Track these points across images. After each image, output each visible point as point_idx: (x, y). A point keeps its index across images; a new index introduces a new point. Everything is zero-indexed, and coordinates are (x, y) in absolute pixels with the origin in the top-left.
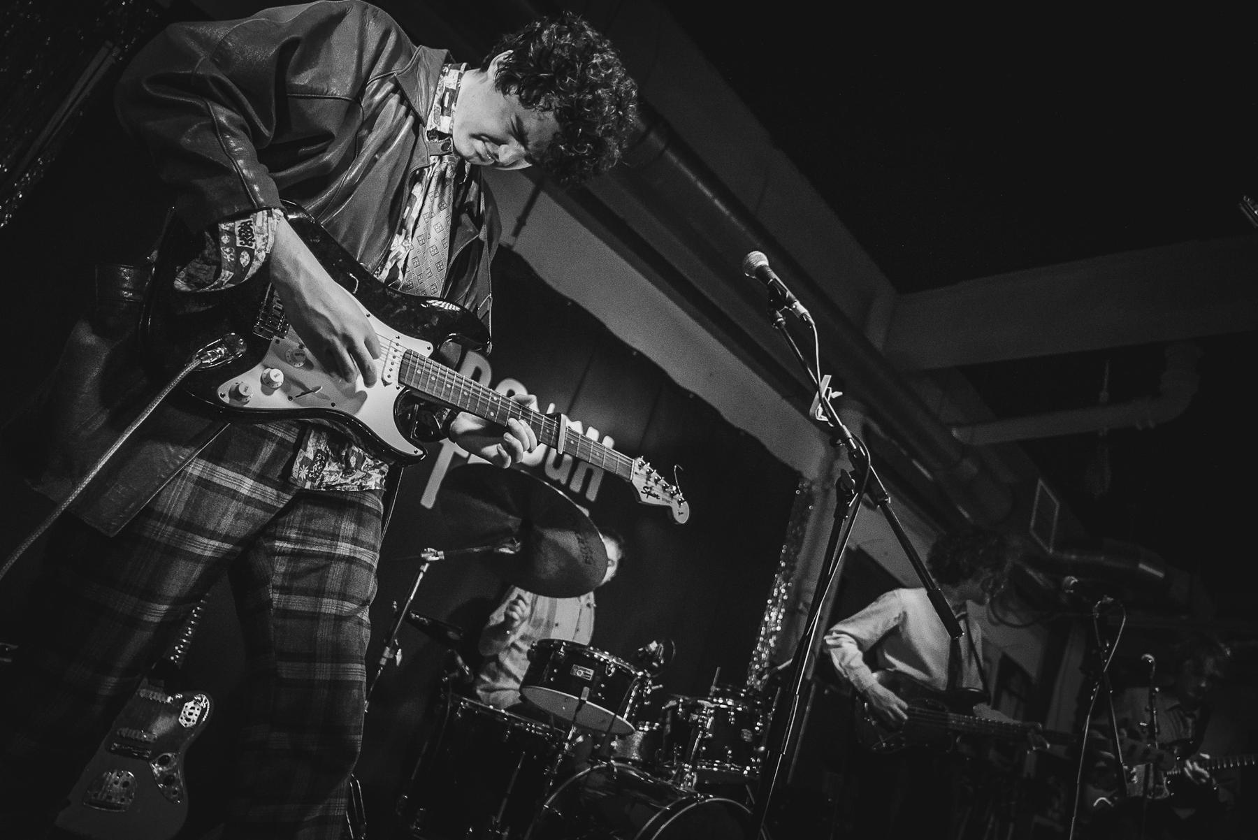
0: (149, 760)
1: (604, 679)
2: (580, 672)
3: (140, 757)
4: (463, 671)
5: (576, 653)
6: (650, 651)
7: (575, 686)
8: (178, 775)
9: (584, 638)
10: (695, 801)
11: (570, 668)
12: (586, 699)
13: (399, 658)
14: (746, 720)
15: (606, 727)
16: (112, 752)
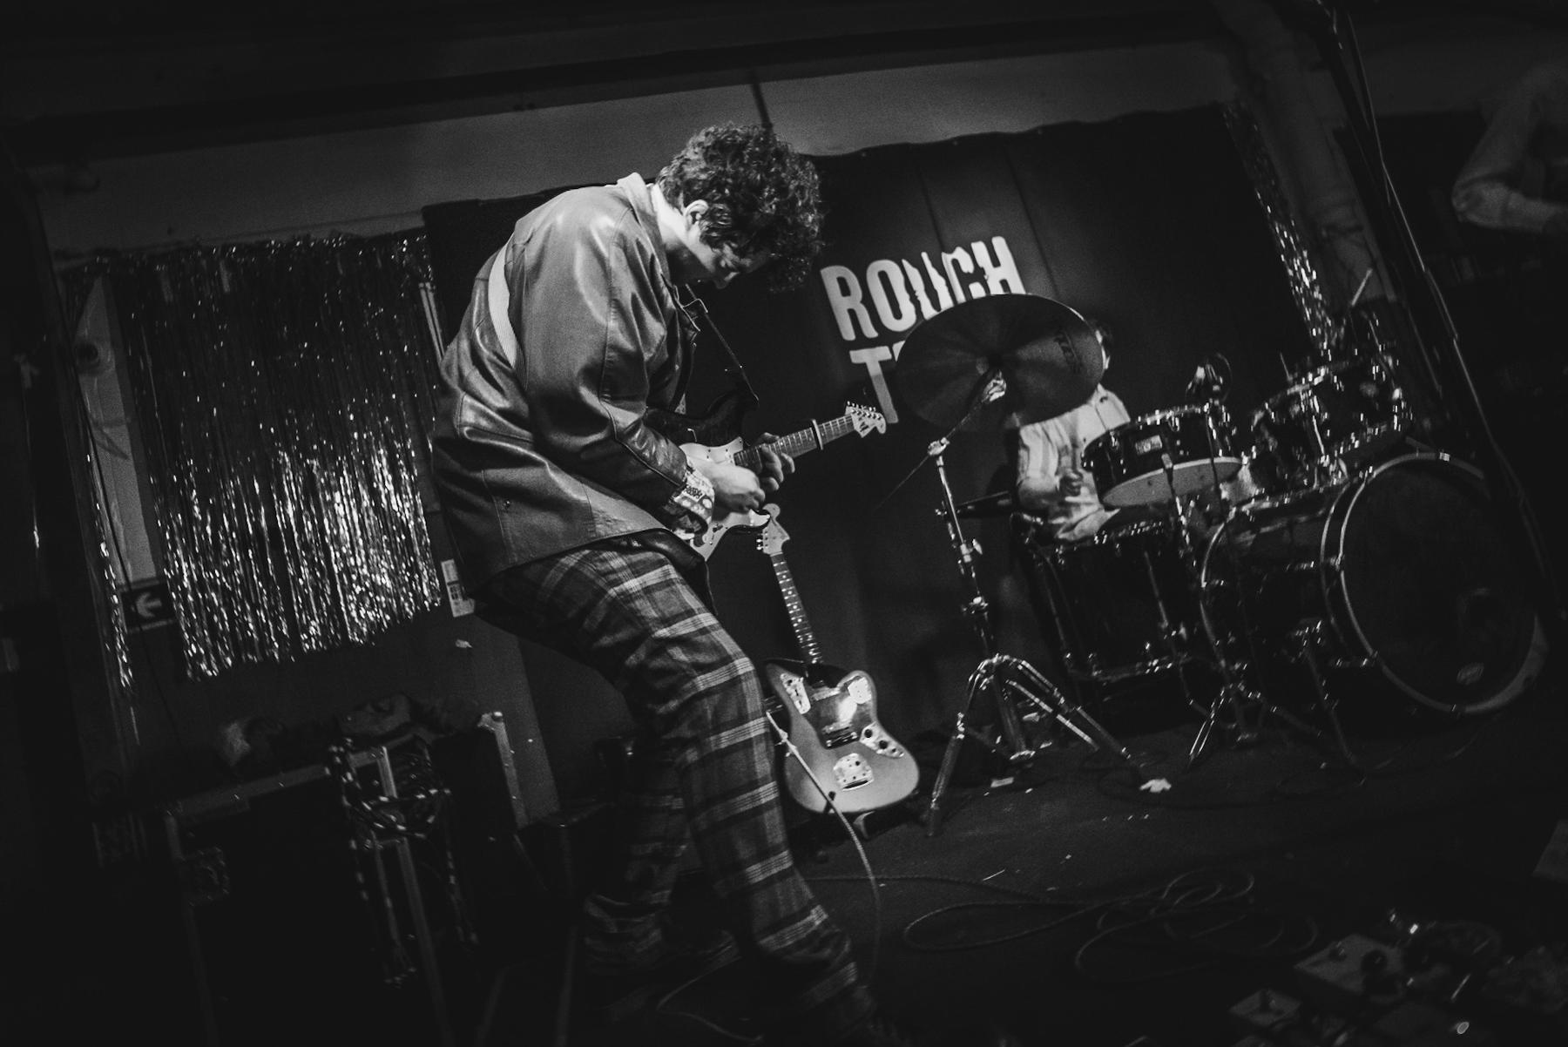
0: (858, 739)
1: (1175, 436)
2: (1146, 447)
3: (850, 740)
4: (1036, 524)
5: (1129, 434)
6: (1201, 380)
7: (1153, 460)
8: (886, 738)
9: (1125, 418)
10: (1361, 481)
11: (1133, 450)
12: (1171, 465)
13: (978, 548)
14: (1355, 374)
15: (1210, 479)
16: (830, 748)
